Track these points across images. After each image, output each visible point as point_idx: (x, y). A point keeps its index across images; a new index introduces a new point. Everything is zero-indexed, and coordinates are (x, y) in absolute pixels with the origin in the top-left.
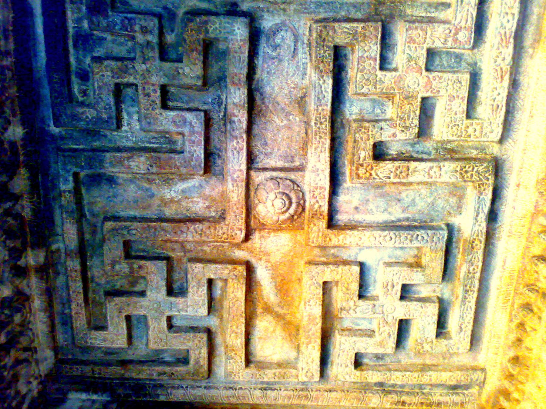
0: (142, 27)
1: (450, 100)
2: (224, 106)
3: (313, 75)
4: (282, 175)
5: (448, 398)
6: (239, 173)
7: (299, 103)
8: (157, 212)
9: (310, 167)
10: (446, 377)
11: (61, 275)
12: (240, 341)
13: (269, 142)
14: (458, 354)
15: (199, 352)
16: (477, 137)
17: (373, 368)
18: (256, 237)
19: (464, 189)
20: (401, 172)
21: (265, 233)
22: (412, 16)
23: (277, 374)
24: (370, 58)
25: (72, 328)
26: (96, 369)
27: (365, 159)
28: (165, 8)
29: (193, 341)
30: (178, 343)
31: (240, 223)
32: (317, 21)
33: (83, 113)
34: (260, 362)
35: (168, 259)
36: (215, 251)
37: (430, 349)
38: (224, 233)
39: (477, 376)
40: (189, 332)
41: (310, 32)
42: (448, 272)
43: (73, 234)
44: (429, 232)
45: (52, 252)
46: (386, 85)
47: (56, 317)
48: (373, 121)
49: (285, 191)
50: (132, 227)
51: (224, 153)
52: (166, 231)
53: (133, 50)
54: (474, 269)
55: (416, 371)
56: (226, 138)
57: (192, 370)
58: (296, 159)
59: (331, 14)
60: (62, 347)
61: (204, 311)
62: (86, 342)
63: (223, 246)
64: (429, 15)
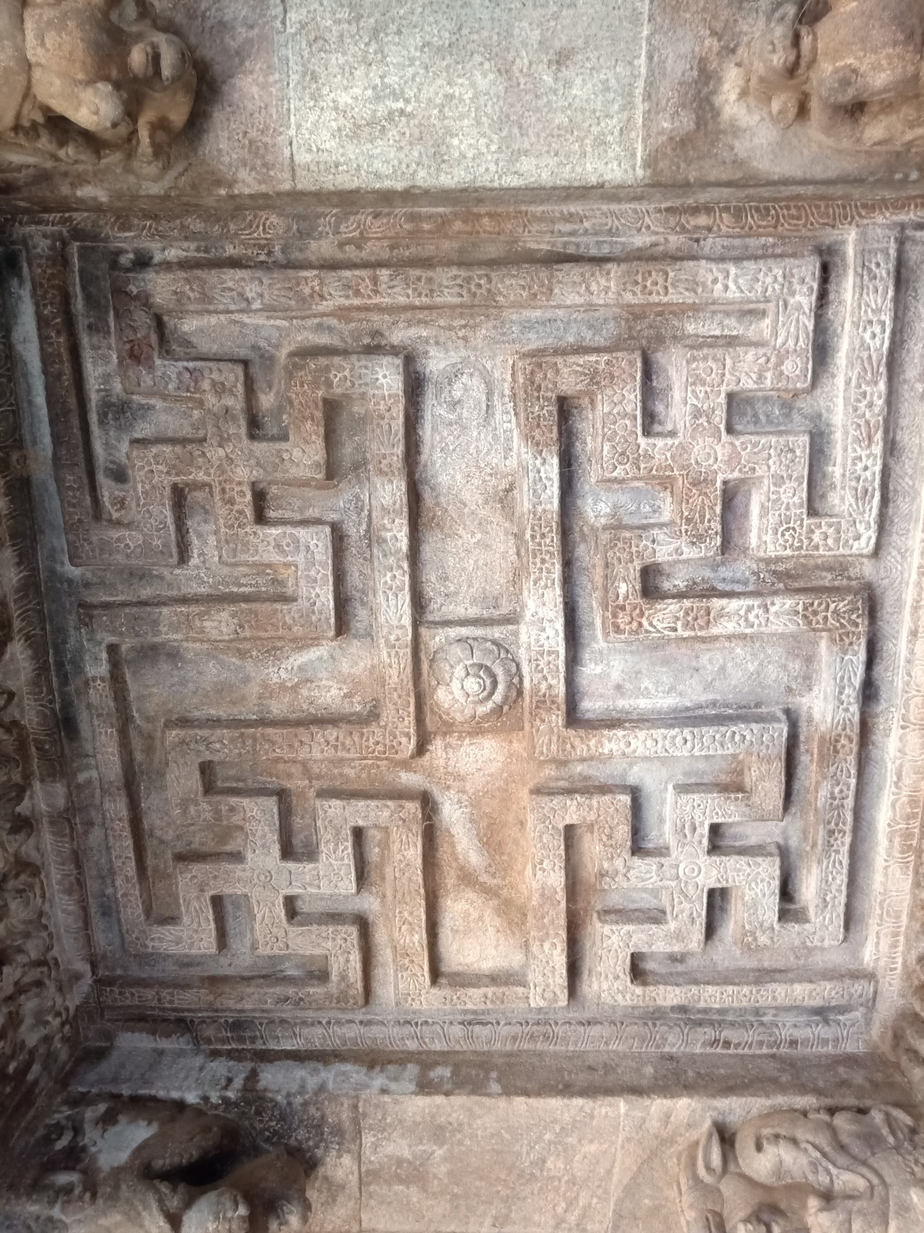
0: (214, 384)
1: (775, 485)
3: (523, 450)
4: (479, 632)
5: (809, 1030)
6: (399, 632)
7: (501, 501)
10: (801, 992)
12: (419, 938)
13: (451, 573)
14: (822, 949)
15: (345, 960)
16: (830, 549)
17: (666, 979)
18: (437, 746)
19: (815, 643)
20: (696, 619)
21: (453, 740)
22: (697, 336)
23: (490, 995)
24: (625, 415)
25: (119, 921)
26: (165, 993)
27: (626, 597)
28: (255, 348)
29: (334, 939)
30: (306, 943)
32: (525, 356)
33: (118, 540)
34: (457, 974)
35: (282, 795)
36: (364, 776)
37: (768, 942)
38: (378, 743)
40: (326, 924)
41: (513, 375)
42: (794, 798)
43: (113, 754)
44: (754, 726)
45: (79, 786)
46: (656, 462)
47: (91, 900)
48: (638, 528)
51: (371, 596)
52: (273, 743)
53: (203, 422)
54: (841, 791)
55: (748, 984)
56: (373, 570)
57: (335, 991)
58: (504, 602)
59: (550, 341)
60: (104, 957)
61: (349, 885)
62: (146, 946)
64: (726, 332)
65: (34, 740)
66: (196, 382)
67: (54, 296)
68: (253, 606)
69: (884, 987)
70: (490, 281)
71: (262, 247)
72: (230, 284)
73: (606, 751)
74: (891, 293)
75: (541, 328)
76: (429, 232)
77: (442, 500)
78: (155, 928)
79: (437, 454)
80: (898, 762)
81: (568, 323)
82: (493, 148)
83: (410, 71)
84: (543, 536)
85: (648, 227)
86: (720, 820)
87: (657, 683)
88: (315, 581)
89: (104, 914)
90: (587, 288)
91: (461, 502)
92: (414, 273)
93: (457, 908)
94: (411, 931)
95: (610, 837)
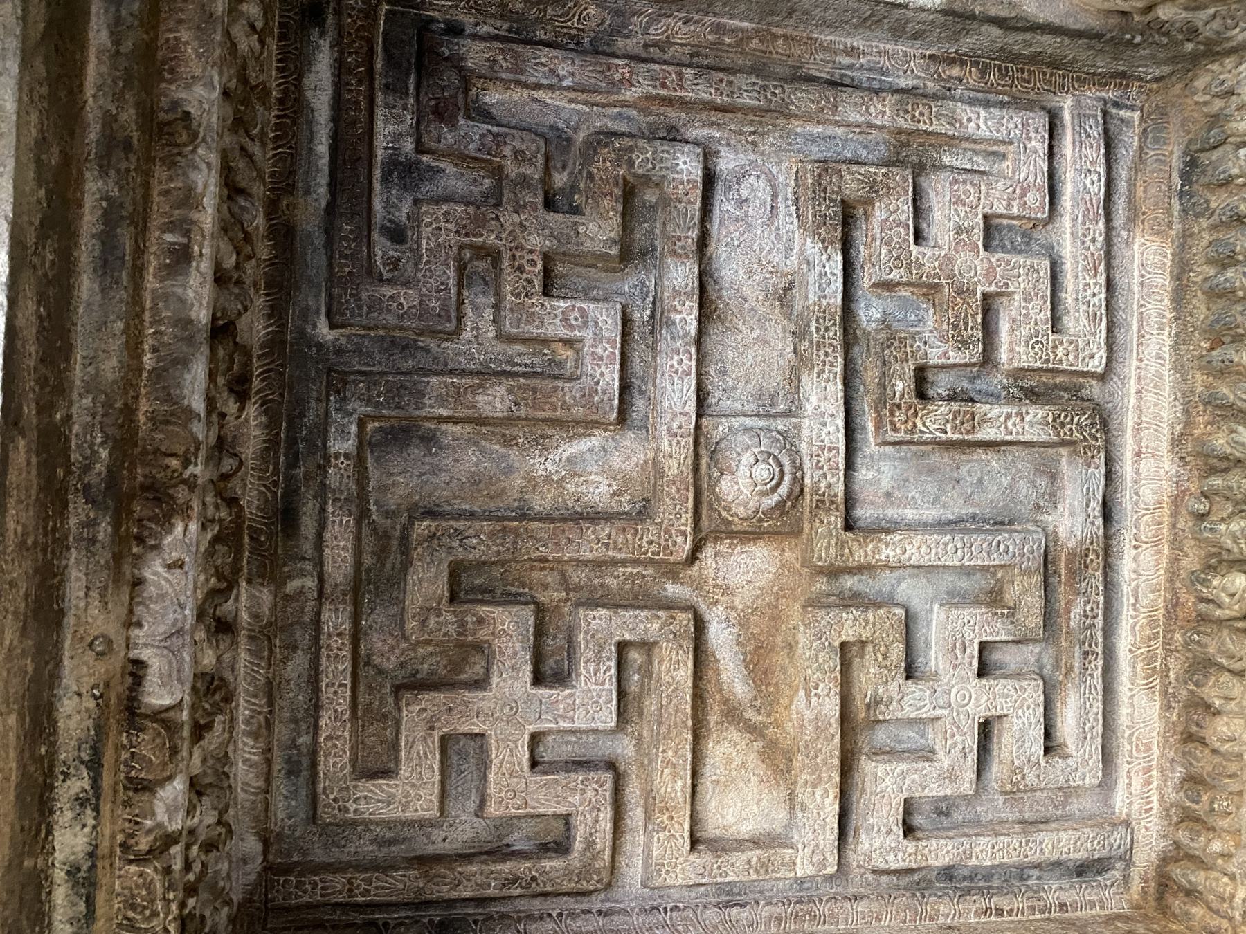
0: (516, 152)
1: (1025, 300)
2: (651, 299)
6: (682, 419)
7: (780, 299)
8: (516, 504)
9: (809, 409)
11: (300, 652)
12: (682, 785)
13: (730, 369)
18: (708, 552)
20: (962, 423)
21: (723, 547)
27: (902, 396)
30: (547, 797)
31: (683, 520)
38: (651, 542)
39: (1118, 838)
40: (576, 771)
45: (287, 598)
46: (926, 269)
50: (471, 532)
51: (650, 385)
54: (1092, 609)
59: (830, 155)
61: (608, 718)
62: (347, 811)
63: (644, 577)
65: (250, 527)
69: (1140, 836)
71: (572, 37)
72: (544, 60)
73: (883, 557)
74: (1102, 151)
76: (729, 45)
77: (724, 293)
78: (362, 783)
79: (722, 248)
80: (1133, 584)
81: (846, 140)
84: (827, 329)
85: (912, 71)
86: (989, 639)
87: (924, 493)
89: (289, 773)
90: (867, 109)
92: (717, 75)
93: (725, 749)
94: (675, 776)
95: (885, 657)
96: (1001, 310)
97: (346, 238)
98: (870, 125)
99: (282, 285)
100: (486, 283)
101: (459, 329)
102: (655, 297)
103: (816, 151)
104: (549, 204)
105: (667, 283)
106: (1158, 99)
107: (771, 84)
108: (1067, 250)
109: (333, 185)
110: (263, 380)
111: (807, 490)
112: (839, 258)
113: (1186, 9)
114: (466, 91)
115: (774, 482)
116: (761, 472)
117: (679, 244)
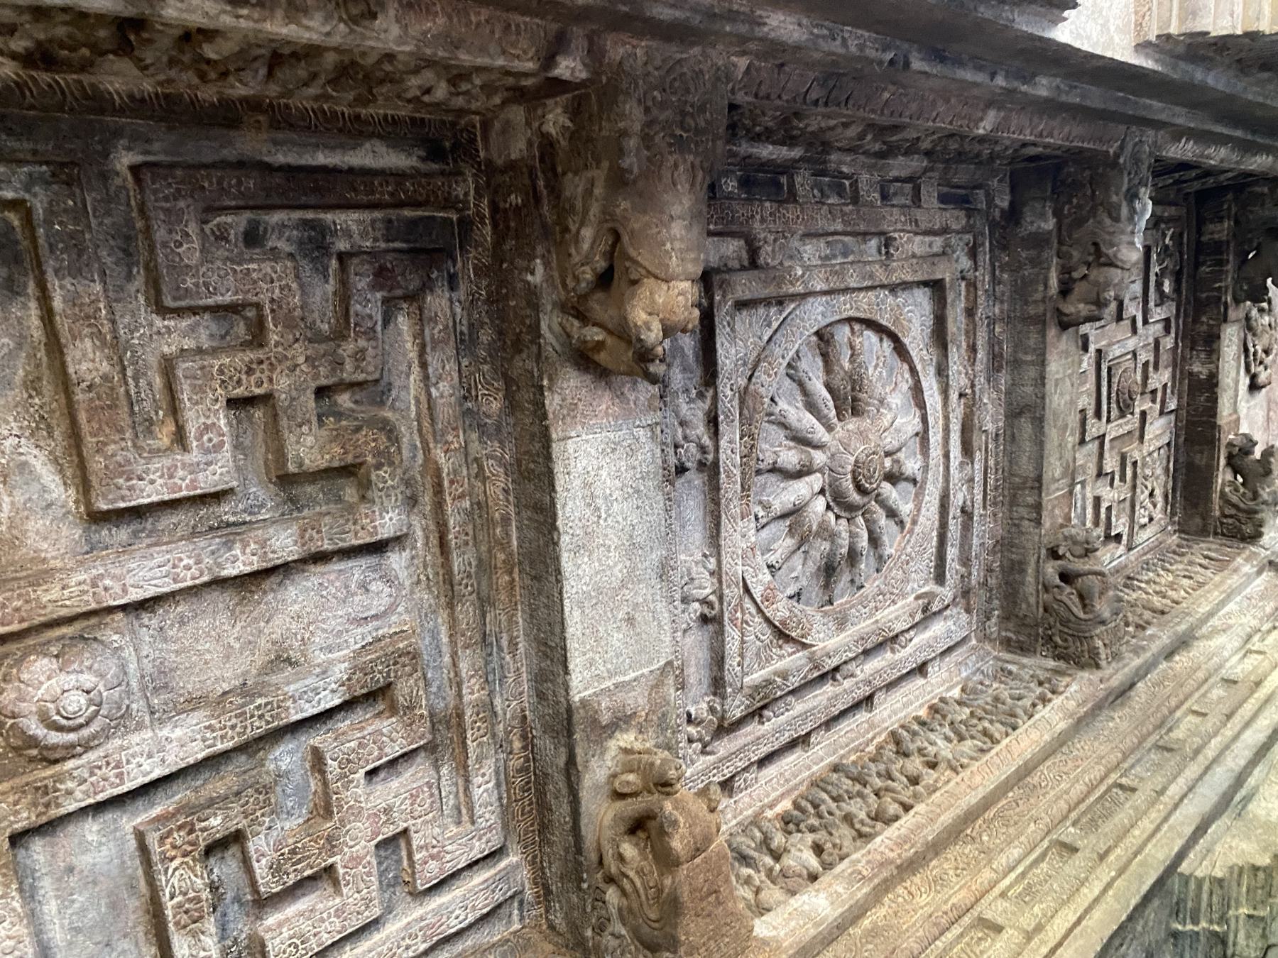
0: (363, 351)
2: (248, 519)
7: (278, 657)
9: (165, 732)
13: (189, 628)
27: (203, 830)
49: (105, 706)
51: (148, 541)
66: (364, 333)
67: (421, 195)
68: (123, 402)
70: (470, 594)
72: (447, 367)
74: (485, 911)
75: (433, 646)
76: (494, 534)
77: (270, 596)
79: (316, 580)
82: (584, 588)
83: (620, 519)
88: (171, 477)
90: (472, 676)
91: (271, 616)
96: (318, 893)
97: (240, 183)
98: (459, 685)
99: (167, 110)
100: (223, 337)
101: (162, 311)
102: (250, 522)
103: (424, 644)
104: (321, 392)
105: (271, 530)
106: (535, 936)
107: (474, 581)
108: (391, 928)
109: (290, 171)
110: (50, 86)
111: (58, 768)
112: (337, 701)
113: (620, 910)
114: (405, 298)
115: (64, 722)
116: (75, 703)
117: (314, 533)
